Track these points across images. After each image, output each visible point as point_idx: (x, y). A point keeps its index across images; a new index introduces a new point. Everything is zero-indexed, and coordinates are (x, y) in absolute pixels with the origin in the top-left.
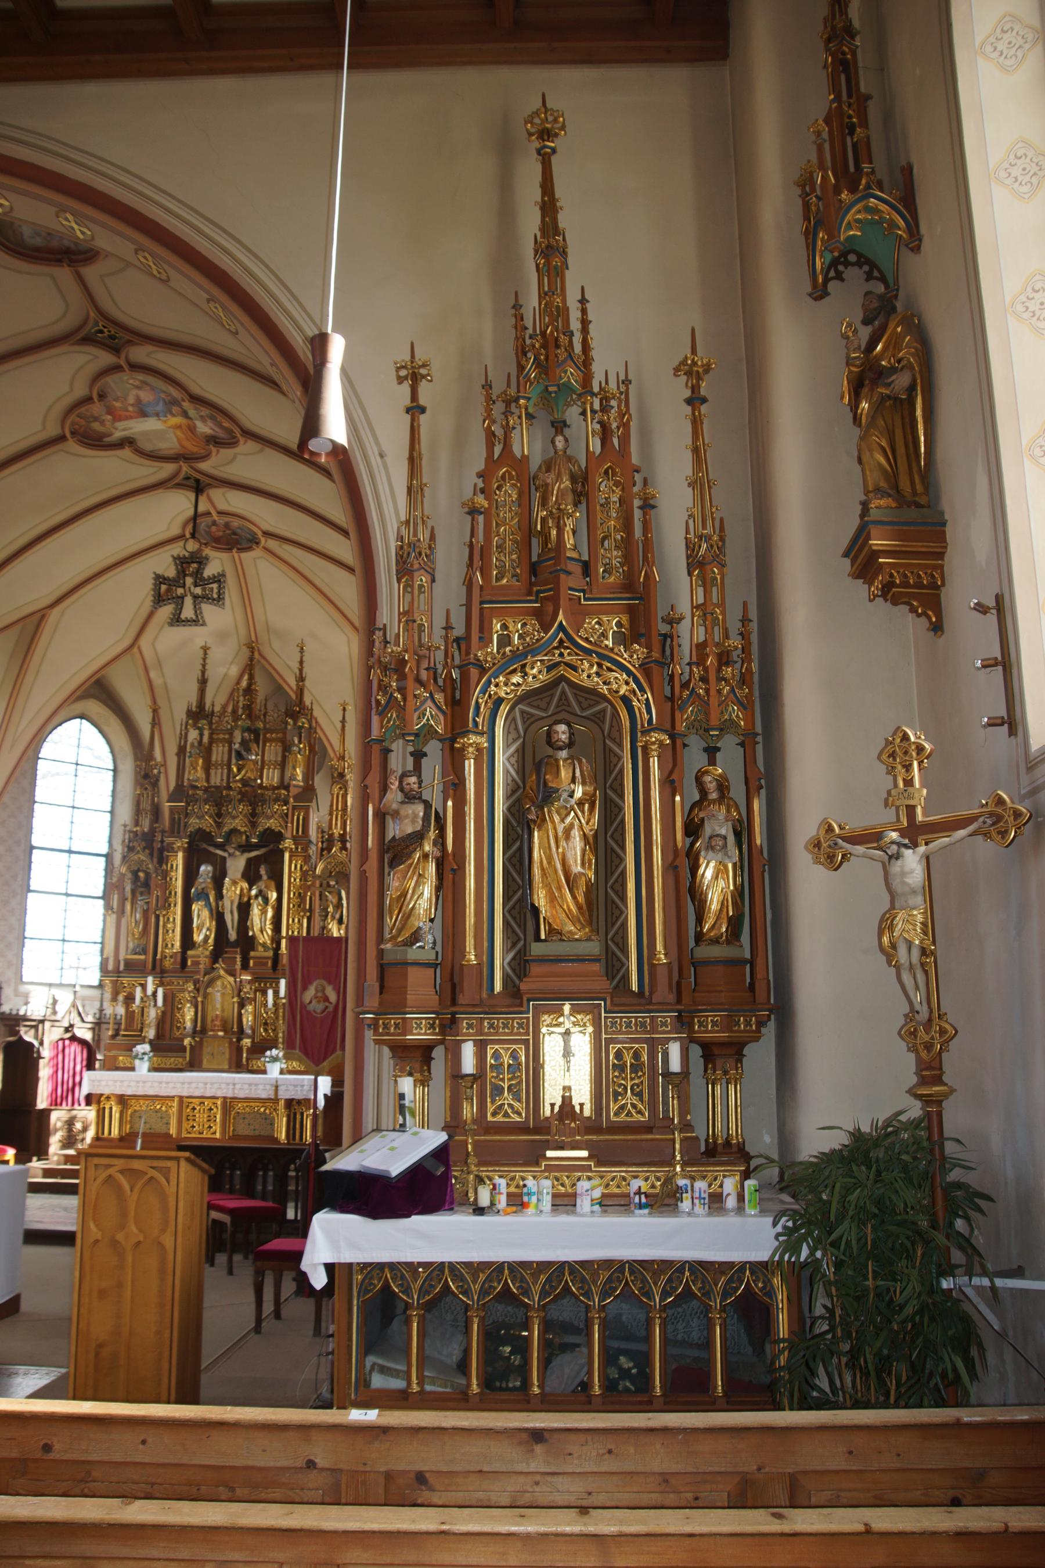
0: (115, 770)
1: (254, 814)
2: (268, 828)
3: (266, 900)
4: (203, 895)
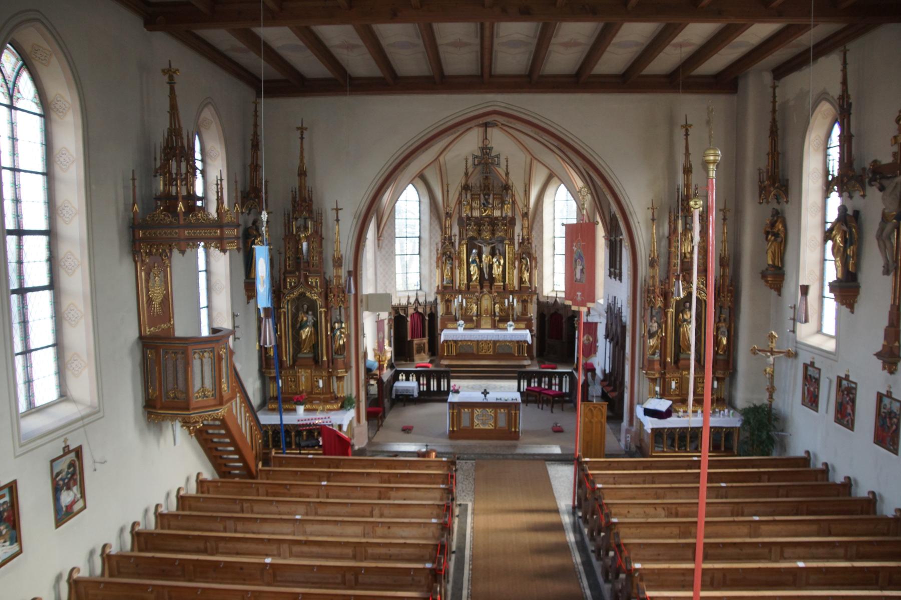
0: (420, 201)
1: (493, 230)
2: (500, 236)
3: (499, 263)
4: (474, 261)
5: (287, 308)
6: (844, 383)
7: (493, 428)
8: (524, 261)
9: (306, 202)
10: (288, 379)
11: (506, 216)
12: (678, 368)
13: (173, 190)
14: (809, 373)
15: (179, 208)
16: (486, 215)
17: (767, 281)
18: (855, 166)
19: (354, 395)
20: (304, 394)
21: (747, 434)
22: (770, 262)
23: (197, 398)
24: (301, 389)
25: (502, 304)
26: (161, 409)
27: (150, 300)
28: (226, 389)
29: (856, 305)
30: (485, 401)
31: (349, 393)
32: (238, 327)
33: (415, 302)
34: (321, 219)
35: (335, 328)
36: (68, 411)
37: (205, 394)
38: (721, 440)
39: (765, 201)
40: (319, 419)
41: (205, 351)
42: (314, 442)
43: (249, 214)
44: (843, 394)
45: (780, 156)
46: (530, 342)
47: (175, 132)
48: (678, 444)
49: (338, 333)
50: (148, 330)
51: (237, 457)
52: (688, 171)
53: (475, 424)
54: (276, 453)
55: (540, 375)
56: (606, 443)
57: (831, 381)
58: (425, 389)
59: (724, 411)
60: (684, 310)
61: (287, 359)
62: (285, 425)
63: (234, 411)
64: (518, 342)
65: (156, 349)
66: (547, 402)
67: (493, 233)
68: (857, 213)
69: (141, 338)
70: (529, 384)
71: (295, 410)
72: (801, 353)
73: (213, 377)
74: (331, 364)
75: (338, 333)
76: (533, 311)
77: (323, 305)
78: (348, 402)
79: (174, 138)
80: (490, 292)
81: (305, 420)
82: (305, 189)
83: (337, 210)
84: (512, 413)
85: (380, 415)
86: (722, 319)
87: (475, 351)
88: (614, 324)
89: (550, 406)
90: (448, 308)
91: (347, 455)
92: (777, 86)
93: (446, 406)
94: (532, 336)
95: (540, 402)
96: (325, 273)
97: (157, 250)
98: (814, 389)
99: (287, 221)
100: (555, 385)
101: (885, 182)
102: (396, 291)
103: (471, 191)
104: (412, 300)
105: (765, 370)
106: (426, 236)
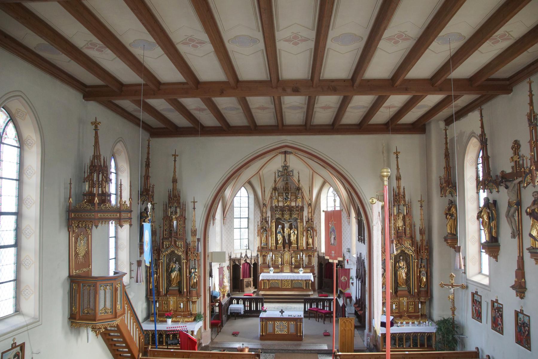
0: (248, 197)
1: (291, 214)
3: (295, 233)
4: (280, 232)
5: (163, 260)
6: (496, 304)
7: (287, 333)
8: (309, 232)
9: (177, 198)
10: (163, 303)
11: (299, 205)
12: (397, 296)
13: (95, 191)
14: (475, 298)
15: (95, 201)
16: (287, 205)
17: (448, 243)
18: (492, 174)
19: (202, 312)
20: (172, 312)
21: (441, 337)
22: (449, 232)
23: (101, 313)
24: (170, 309)
25: (296, 258)
26: (79, 320)
27: (77, 254)
28: (119, 308)
29: (498, 257)
30: (282, 317)
31: (200, 311)
32: (133, 271)
33: (245, 256)
34: (185, 208)
35: (191, 272)
36: (19, 320)
37: (106, 311)
38: (425, 341)
39: (444, 195)
40: (180, 327)
41: (108, 285)
42: (176, 341)
43: (143, 204)
44: (495, 312)
45: (451, 169)
46: (313, 280)
47: (97, 157)
48: (399, 343)
49: (193, 275)
50: (74, 272)
51: (127, 350)
52: (398, 178)
53: (276, 331)
54: (151, 348)
55: (317, 301)
56: (355, 342)
57: (487, 303)
58: (248, 309)
59: (426, 323)
60: (399, 261)
61: (163, 290)
62: (158, 330)
63: (126, 322)
64: (306, 280)
65: (78, 283)
66: (321, 317)
67: (291, 215)
68: (495, 202)
69: (70, 276)
70: (311, 306)
71: (166, 321)
72: (470, 286)
73: (112, 301)
74: (188, 294)
75: (193, 275)
76: (315, 262)
77: (185, 259)
78: (199, 317)
79: (96, 160)
80: (289, 251)
81: (171, 328)
82: (176, 190)
83: (194, 202)
84: (298, 324)
85: (219, 325)
86: (422, 266)
87: (280, 286)
88: (360, 269)
89: (323, 319)
90: (264, 260)
91: (195, 350)
92: (448, 129)
93: (259, 319)
94: (314, 277)
95: (317, 317)
96: (186, 239)
97: (82, 224)
98: (479, 308)
99: (165, 209)
100: (327, 306)
101: (508, 184)
102: (234, 250)
103: (278, 191)
104: (243, 255)
105: (449, 297)
106: (252, 217)
